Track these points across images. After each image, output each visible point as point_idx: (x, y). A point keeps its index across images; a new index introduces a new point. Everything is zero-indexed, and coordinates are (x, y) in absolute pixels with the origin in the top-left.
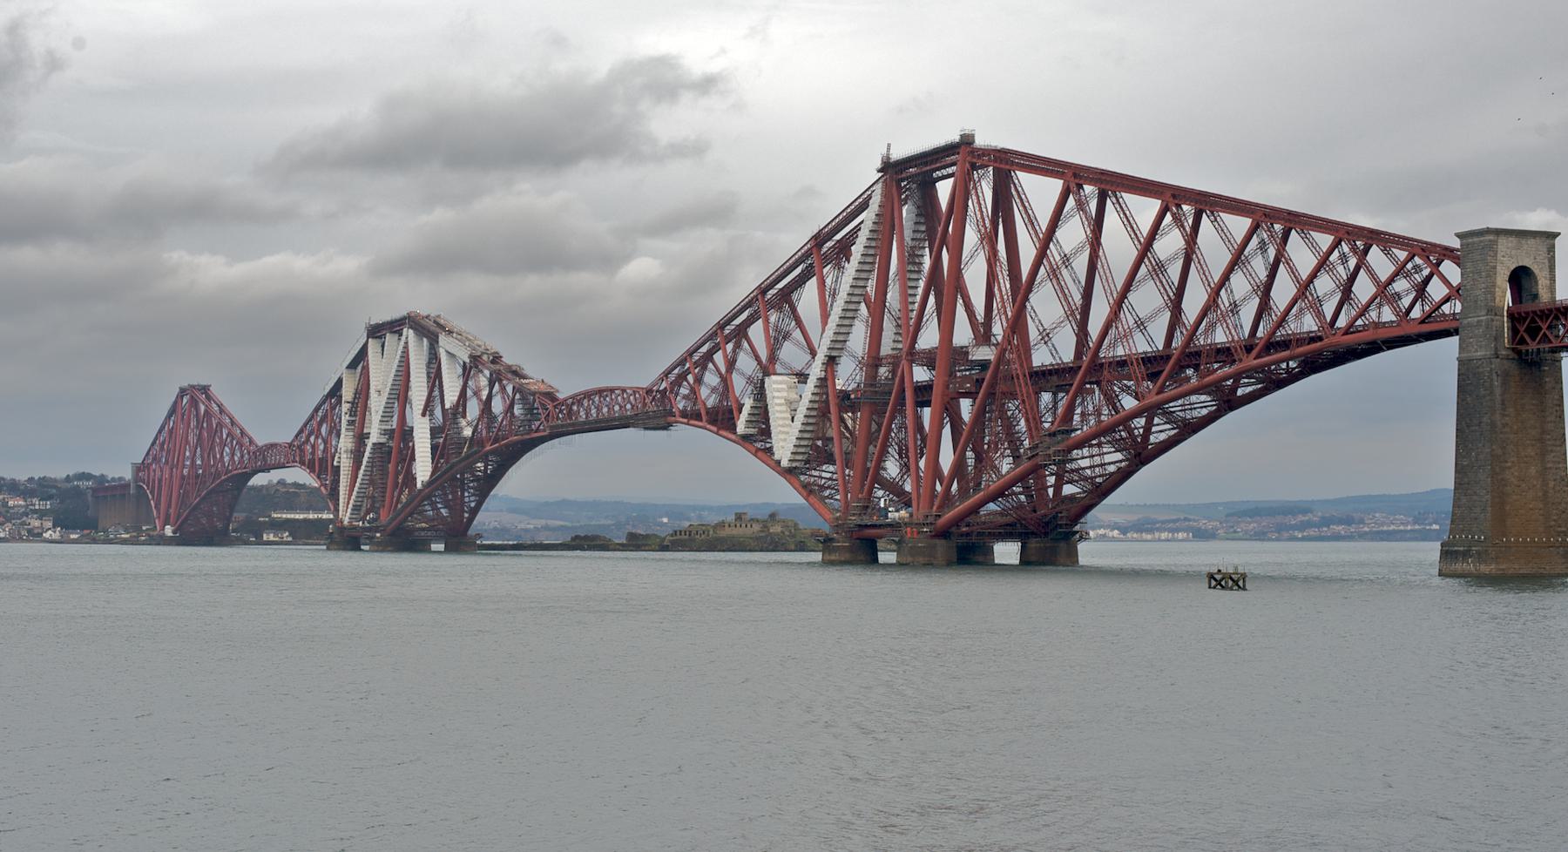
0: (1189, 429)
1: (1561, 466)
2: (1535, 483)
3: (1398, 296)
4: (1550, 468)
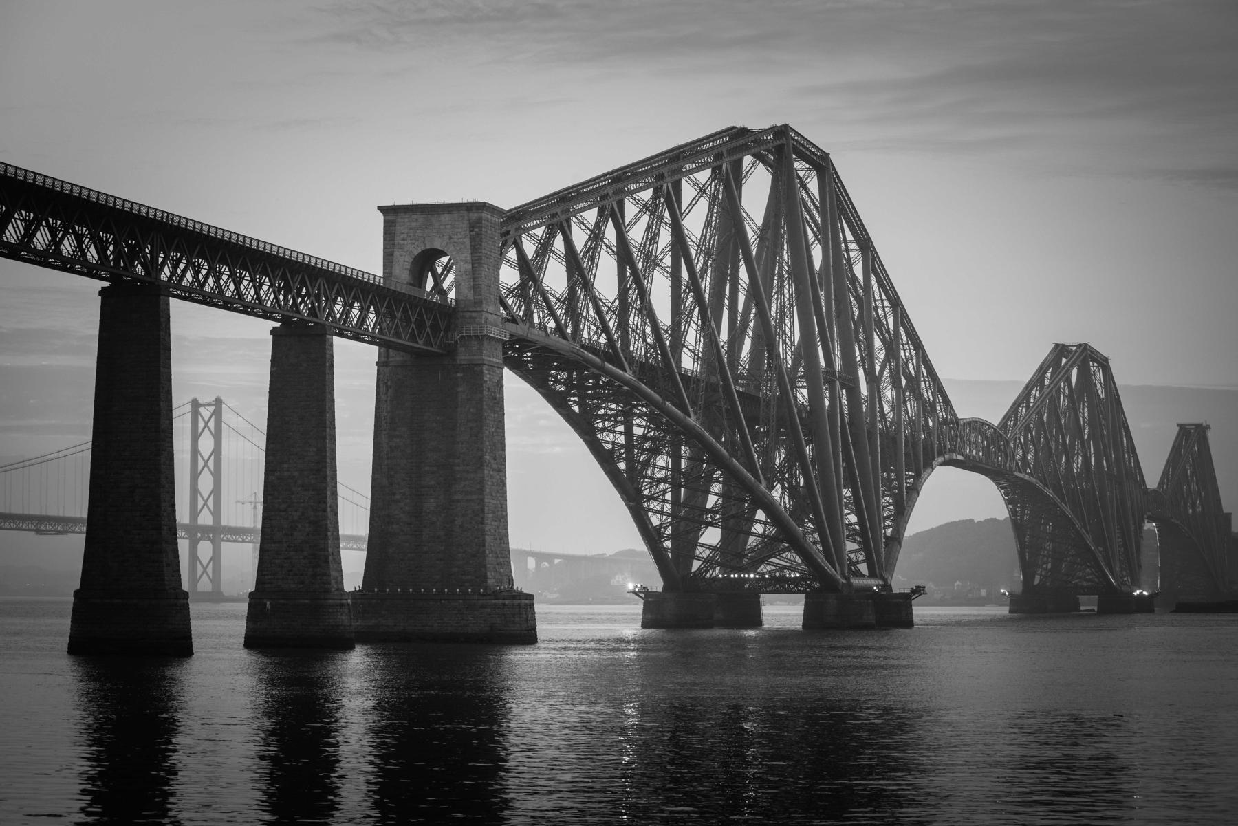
1: (474, 497)
2: (435, 519)
4: (458, 501)
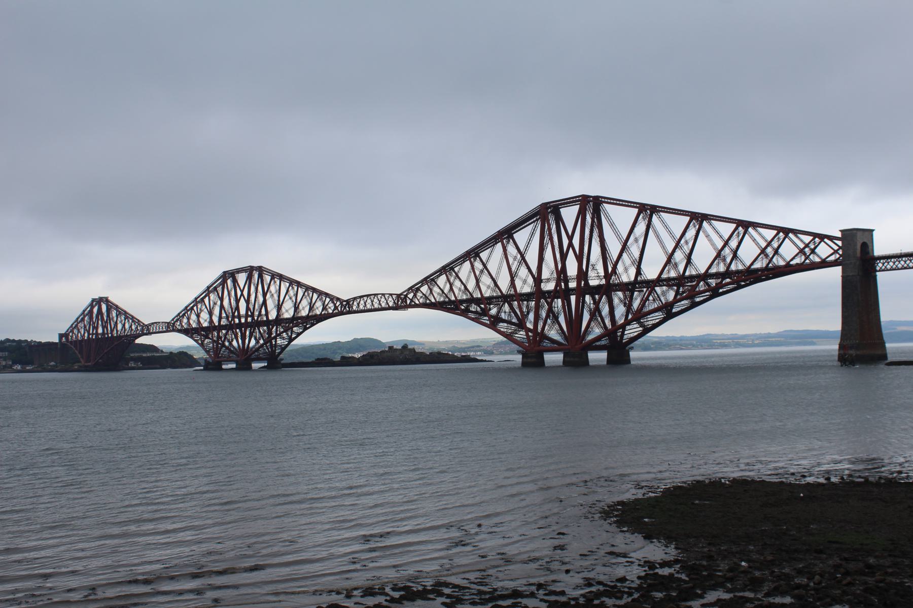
0: (299, 334)
3: (330, 308)
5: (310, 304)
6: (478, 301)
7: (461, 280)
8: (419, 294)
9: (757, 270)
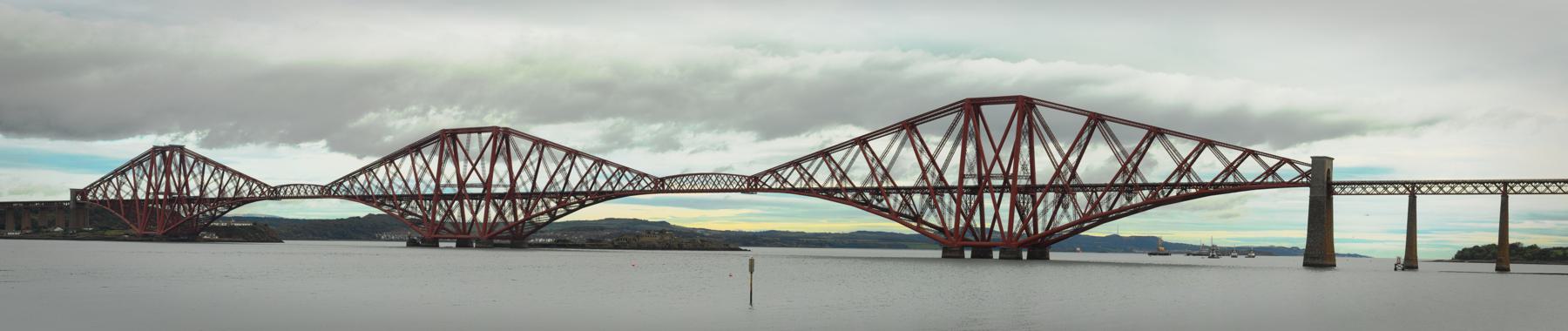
5: (237, 187)
6: (391, 198)
7: (378, 180)
8: (342, 188)
9: (605, 192)
